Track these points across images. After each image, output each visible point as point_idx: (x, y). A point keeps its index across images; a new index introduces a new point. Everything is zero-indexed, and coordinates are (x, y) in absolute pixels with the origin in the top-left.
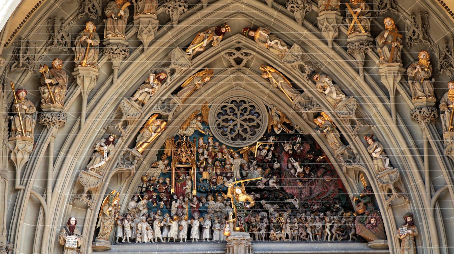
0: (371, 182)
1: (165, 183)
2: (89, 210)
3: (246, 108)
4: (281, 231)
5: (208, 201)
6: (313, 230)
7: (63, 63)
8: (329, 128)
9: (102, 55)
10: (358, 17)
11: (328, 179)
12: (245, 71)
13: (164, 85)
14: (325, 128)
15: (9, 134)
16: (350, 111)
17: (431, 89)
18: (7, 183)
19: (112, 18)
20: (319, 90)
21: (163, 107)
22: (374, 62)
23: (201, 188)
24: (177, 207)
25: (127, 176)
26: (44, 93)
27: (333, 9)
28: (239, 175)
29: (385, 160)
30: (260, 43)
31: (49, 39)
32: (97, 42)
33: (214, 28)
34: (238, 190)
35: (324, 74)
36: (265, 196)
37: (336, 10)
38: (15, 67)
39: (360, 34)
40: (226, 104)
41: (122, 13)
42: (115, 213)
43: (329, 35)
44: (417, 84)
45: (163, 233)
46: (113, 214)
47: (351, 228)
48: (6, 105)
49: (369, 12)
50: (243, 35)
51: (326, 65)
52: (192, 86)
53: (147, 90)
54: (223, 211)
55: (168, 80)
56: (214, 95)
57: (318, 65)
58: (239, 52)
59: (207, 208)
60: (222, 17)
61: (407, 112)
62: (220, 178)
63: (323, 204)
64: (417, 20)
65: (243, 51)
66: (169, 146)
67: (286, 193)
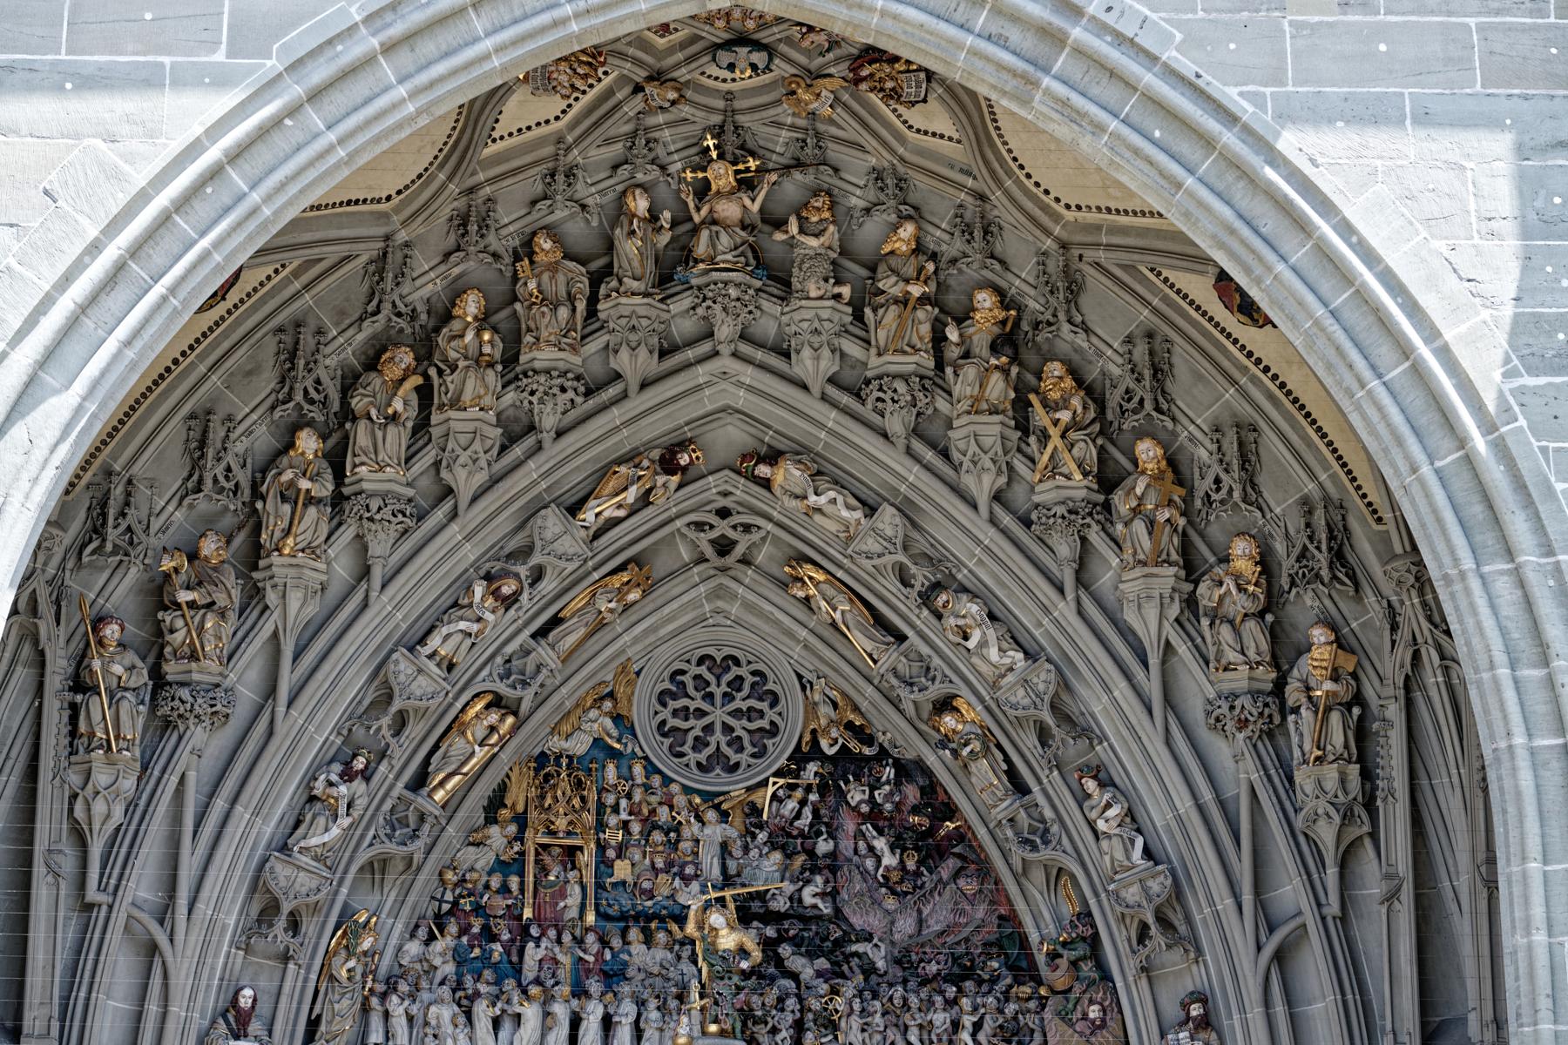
0: (1092, 902)
1: (505, 890)
2: (291, 966)
3: (740, 679)
4: (836, 1038)
5: (629, 943)
6: (925, 1037)
7: (228, 542)
8: (976, 745)
9: (340, 524)
10: (1063, 436)
11: (969, 886)
12: (740, 575)
13: (512, 612)
14: (966, 745)
15: (71, 744)
16: (1038, 701)
17: (1264, 646)
18: (63, 885)
19: (370, 419)
20: (951, 637)
21: (508, 674)
22: (1106, 561)
23: (609, 905)
24: (540, 961)
25: (401, 867)
26: (172, 631)
27: (994, 411)
28: (716, 872)
29: (1132, 842)
30: (786, 499)
31: (191, 476)
32: (324, 489)
33: (656, 454)
34: (716, 919)
35: (965, 590)
36: (792, 933)
37: (1003, 412)
38: (93, 553)
39: (1069, 483)
40: (684, 666)
41: (398, 405)
42: (364, 975)
43: (982, 485)
44: (1225, 632)
45: (501, 1035)
46: (358, 977)
47: (1032, 1031)
48: (64, 663)
49: (1093, 422)
50: (739, 473)
52: (590, 617)
53: (463, 625)
54: (671, 975)
55: (525, 596)
56: (652, 638)
59: (626, 964)
60: (682, 421)
61: (1195, 709)
62: (662, 877)
63: (956, 959)
64: (1225, 446)
65: (735, 519)
66: (520, 782)
67: (851, 925)
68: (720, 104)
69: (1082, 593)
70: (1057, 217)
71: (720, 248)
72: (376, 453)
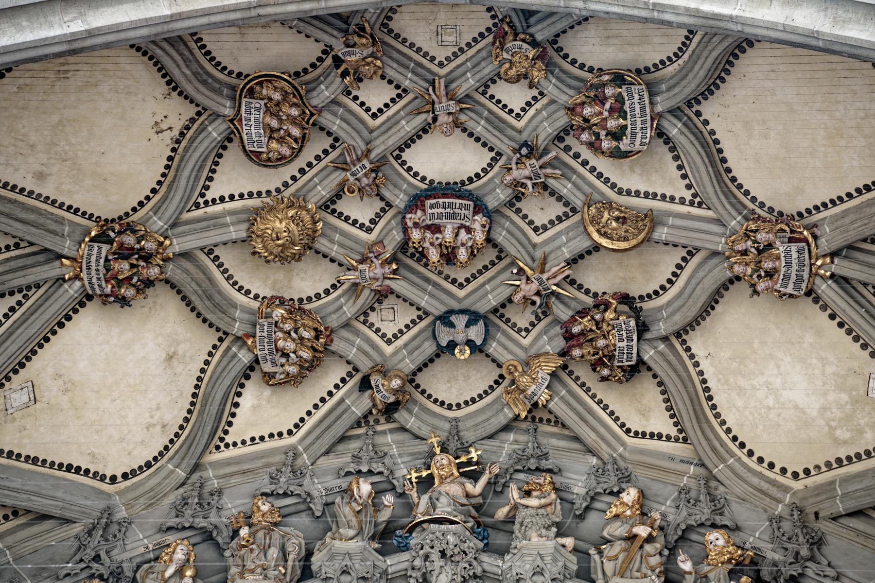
68: (447, 426)
70: (786, 489)
71: (439, 505)
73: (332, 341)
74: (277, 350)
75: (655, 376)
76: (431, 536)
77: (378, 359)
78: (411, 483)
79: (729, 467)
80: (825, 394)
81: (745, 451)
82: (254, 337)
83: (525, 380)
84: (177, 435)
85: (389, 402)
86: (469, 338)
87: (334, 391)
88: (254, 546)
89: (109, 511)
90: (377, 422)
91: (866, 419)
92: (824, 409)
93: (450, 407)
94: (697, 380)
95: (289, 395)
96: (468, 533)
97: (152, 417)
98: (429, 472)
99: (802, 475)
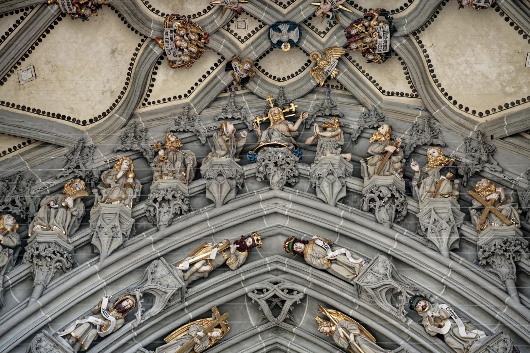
13: (129, 325)
19: (50, 208)
39: (502, 228)
51: (440, 295)
55: (140, 312)
57: (425, 293)
58: (276, 286)
69: (521, 295)
70: (475, 123)
71: (273, 136)
72: (49, 222)
73: (209, 41)
74: (176, 47)
75: (400, 59)
76: (269, 154)
77: (236, 51)
78: (257, 124)
79: (442, 111)
80: (500, 66)
81: (452, 101)
82: (162, 39)
83: (323, 63)
84: (120, 97)
85: (243, 77)
86: (290, 38)
87: (211, 71)
88: (167, 161)
89: (83, 141)
90: (236, 89)
91: (524, 81)
92: (499, 75)
93: (279, 80)
94: (424, 60)
95: (184, 73)
96: (290, 152)
97: (104, 87)
98: (267, 118)
99: (484, 114)
